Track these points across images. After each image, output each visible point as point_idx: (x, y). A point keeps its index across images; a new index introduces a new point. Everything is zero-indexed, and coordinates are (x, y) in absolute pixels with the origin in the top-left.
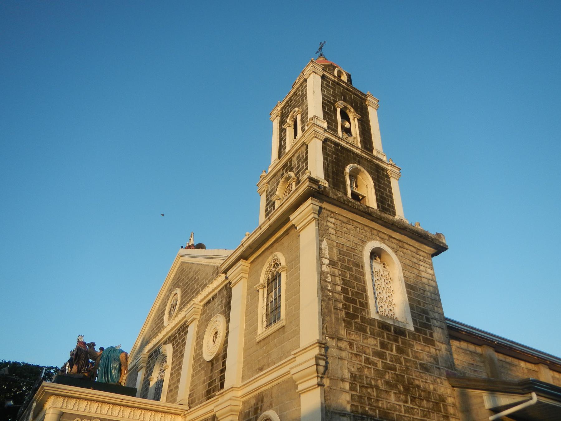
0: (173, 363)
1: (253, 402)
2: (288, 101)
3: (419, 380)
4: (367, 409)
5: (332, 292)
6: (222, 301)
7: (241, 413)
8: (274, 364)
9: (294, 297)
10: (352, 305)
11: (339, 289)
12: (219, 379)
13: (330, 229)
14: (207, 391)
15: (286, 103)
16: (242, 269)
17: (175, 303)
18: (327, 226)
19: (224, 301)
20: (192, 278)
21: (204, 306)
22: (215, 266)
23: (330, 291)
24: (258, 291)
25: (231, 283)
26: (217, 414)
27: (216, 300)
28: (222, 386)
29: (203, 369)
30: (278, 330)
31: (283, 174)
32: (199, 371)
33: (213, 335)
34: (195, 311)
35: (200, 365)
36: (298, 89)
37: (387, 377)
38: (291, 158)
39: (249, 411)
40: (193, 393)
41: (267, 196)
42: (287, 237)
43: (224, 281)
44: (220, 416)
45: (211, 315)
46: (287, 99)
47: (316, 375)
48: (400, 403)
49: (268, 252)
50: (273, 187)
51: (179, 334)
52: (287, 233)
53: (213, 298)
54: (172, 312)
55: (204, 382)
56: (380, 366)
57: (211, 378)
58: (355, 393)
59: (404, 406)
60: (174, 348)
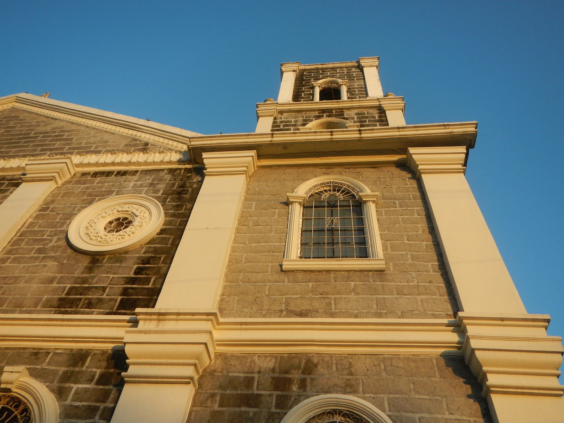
1: (270, 364)
2: (317, 69)
7: (207, 374)
8: (356, 316)
12: (119, 291)
14: (60, 299)
15: (314, 69)
16: (249, 163)
19: (162, 187)
20: (47, 133)
21: (84, 174)
22: (135, 140)
24: (287, 204)
25: (206, 169)
26: (128, 349)
30: (361, 271)
31: (322, 116)
32: (37, 258)
34: (61, 169)
35: (39, 251)
36: (340, 68)
38: (342, 109)
39: (249, 382)
41: (274, 122)
42: (372, 170)
43: (170, 162)
45: (109, 193)
46: (320, 66)
49: (318, 170)
50: (293, 120)
52: (374, 165)
53: (124, 173)
55: (51, 281)
57: (84, 281)
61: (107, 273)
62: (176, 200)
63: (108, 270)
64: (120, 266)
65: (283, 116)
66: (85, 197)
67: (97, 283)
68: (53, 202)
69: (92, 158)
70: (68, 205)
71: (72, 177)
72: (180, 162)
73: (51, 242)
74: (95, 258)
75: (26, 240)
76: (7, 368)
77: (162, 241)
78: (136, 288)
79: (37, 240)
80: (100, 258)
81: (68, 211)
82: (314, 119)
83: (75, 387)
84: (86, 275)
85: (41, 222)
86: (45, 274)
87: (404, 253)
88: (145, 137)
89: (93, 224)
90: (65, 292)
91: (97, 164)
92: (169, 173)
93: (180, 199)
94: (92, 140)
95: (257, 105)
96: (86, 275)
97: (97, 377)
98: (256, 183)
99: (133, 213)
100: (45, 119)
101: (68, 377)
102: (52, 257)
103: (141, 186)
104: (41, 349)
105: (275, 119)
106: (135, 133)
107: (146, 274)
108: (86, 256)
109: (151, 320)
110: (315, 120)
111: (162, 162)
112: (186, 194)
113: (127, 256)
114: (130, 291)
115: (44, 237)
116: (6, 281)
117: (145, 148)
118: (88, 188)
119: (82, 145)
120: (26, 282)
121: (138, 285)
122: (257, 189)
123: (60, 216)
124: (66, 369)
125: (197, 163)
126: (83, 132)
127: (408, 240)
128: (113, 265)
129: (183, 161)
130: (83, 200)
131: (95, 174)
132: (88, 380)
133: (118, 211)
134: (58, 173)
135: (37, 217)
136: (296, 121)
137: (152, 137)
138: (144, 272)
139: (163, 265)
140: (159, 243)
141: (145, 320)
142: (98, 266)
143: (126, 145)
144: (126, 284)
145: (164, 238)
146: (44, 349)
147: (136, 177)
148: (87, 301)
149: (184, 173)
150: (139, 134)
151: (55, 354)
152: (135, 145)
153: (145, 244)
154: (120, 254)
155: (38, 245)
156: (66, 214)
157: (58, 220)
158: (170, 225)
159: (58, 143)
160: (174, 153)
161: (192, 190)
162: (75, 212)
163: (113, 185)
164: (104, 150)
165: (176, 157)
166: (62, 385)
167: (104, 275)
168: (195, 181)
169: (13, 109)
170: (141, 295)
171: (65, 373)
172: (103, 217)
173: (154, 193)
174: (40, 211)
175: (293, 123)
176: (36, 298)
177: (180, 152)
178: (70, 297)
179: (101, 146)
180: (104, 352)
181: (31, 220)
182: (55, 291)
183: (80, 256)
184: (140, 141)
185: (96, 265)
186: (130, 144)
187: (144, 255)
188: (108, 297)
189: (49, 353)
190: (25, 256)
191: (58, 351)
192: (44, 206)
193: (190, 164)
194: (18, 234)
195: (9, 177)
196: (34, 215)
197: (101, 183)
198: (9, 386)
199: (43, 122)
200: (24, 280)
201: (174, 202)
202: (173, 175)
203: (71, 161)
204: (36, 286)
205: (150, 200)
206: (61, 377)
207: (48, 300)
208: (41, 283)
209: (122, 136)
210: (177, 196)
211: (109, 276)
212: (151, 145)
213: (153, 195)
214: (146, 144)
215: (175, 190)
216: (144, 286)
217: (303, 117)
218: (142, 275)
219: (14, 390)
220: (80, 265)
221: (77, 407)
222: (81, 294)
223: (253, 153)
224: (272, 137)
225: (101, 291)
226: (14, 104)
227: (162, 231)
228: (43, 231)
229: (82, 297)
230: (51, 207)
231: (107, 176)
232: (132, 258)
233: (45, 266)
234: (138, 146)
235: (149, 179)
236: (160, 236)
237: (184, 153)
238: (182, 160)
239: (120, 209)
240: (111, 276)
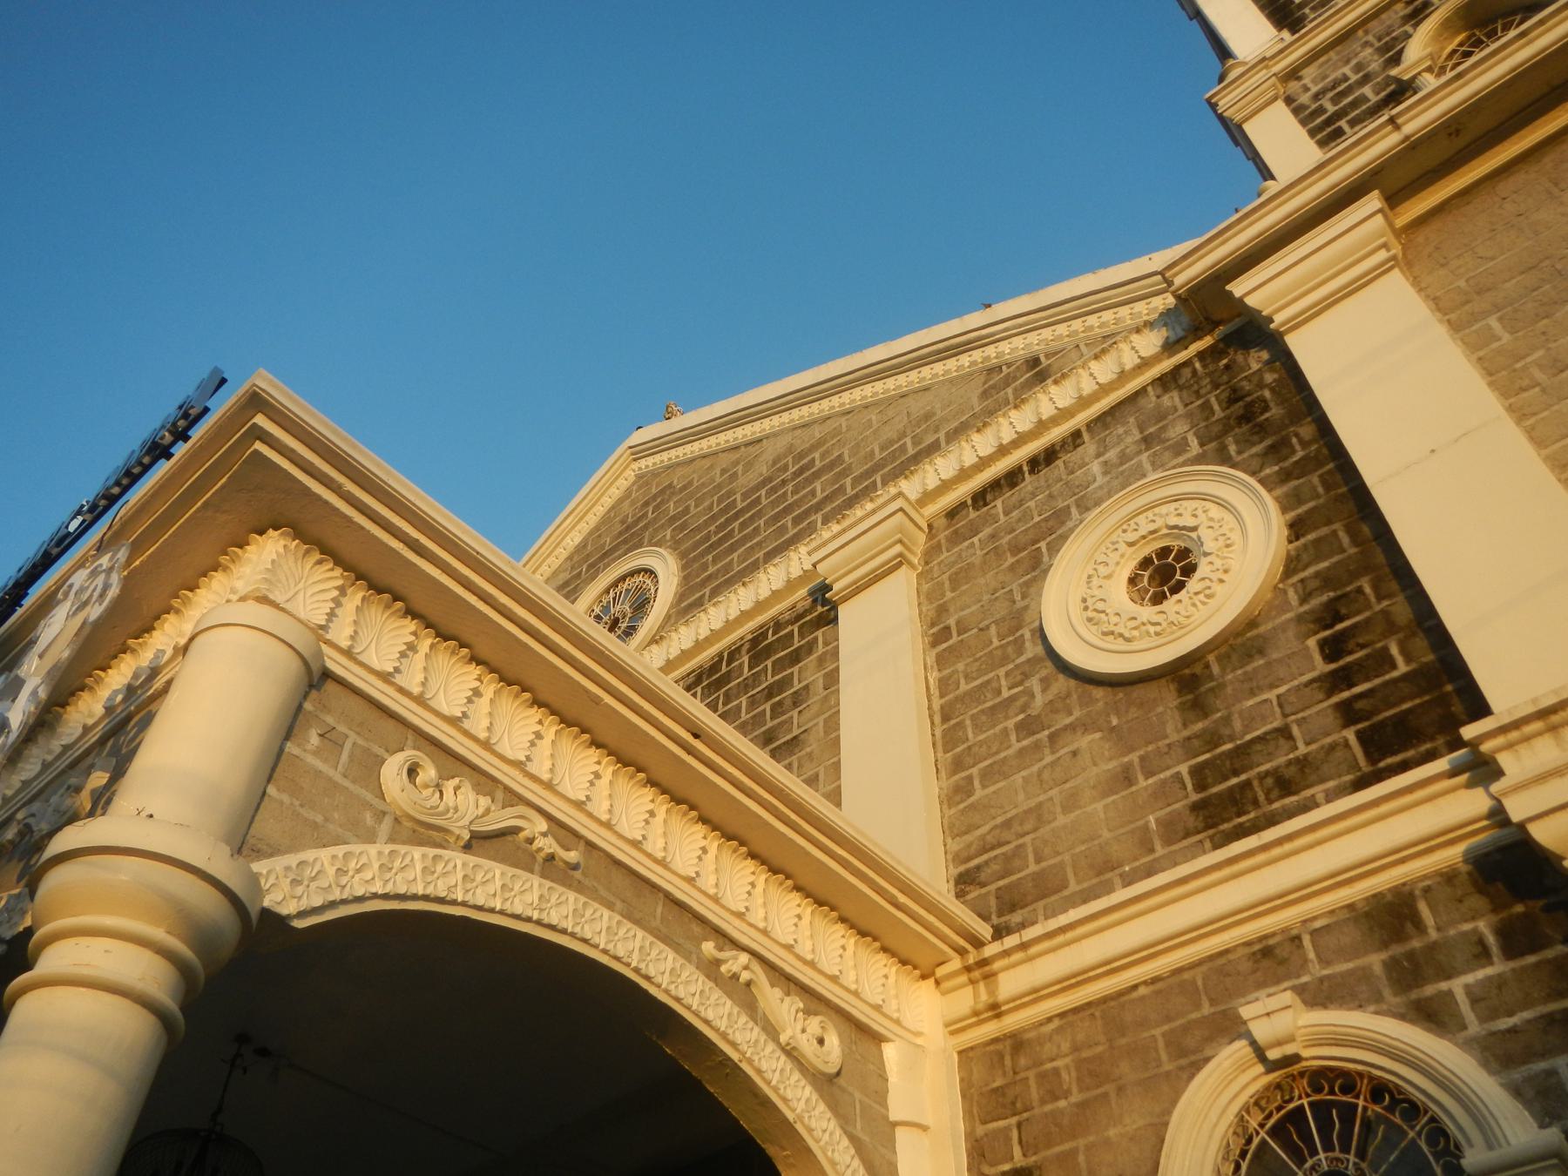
14: (1196, 807)
21: (952, 514)
29: (1084, 726)
32: (1037, 746)
35: (1026, 728)
43: (1145, 364)
45: (1061, 516)
53: (1049, 456)
55: (1126, 778)
61: (1252, 693)
62: (1256, 438)
63: (1246, 686)
64: (1269, 664)
65: (1306, 81)
66: (1011, 560)
67: (1247, 728)
68: (942, 610)
69: (943, 466)
70: (986, 597)
72: (1170, 347)
73: (1033, 696)
74: (1186, 677)
75: (968, 722)
77: (1320, 549)
78: (1371, 692)
79: (993, 708)
80: (1198, 669)
81: (1001, 609)
82: (1408, 28)
85: (960, 666)
86: (1095, 770)
88: (1015, 348)
89: (1100, 606)
90: (1190, 786)
91: (964, 474)
92: (1166, 389)
93: (1262, 430)
94: (889, 433)
95: (1208, 101)
97: (1491, 940)
98: (1442, 272)
99: (1175, 527)
100: (734, 456)
102: (1072, 728)
103: (1124, 458)
104: (1266, 937)
105: (1289, 101)
106: (977, 355)
107: (1363, 646)
108: (1154, 684)
109: (1527, 739)
110: (1416, 26)
111: (1123, 376)
112: (1266, 409)
113: (1262, 629)
114: (1359, 705)
115: (1006, 694)
116: (1017, 828)
117: (1038, 371)
118: (993, 536)
119: (878, 456)
120: (1066, 809)
121: (1368, 679)
122: (1462, 283)
123: (993, 629)
124: (1384, 955)
125: (1217, 324)
126: (849, 428)
128: (1249, 668)
129: (1178, 341)
130: (1012, 568)
131: (980, 498)
132: (1476, 956)
133: (1131, 544)
134: (900, 541)
135: (941, 661)
136: (1359, 67)
137: (1033, 338)
138: (1351, 645)
139: (1385, 603)
140: (1318, 558)
141: (1510, 746)
142: (1212, 689)
143: (985, 394)
145: (1317, 541)
146: (1273, 934)
147: (1089, 447)
148: (1269, 781)
149: (1204, 366)
150: (991, 351)
151: (1314, 933)
152: (1007, 381)
153: (1282, 580)
154: (1238, 634)
155: (1007, 718)
156: (1003, 619)
157: (996, 643)
158: (1300, 502)
159: (818, 485)
160: (1135, 337)
161: (1272, 390)
162: (1020, 604)
163: (1051, 496)
164: (942, 435)
165: (1150, 343)
166: (1414, 995)
167: (1250, 703)
168: (1255, 366)
169: (642, 479)
170: (1403, 700)
172: (1108, 577)
173: (1178, 454)
174: (934, 644)
175: (1354, 78)
176: (1132, 832)
177: (1150, 325)
178: (1215, 790)
179: (926, 431)
180: (1449, 876)
181: (933, 677)
182: (1161, 794)
183: (1138, 692)
184: (1009, 365)
185: (1202, 689)
186: (992, 387)
187: (1306, 607)
188: (1314, 747)
189: (1298, 938)
190: (1002, 755)
191: (1318, 924)
192: (935, 630)
193: (1200, 338)
194: (937, 719)
195: (787, 616)
196: (931, 660)
197: (1015, 508)
198: (1289, 1049)
199: (737, 463)
200: (1059, 809)
201: (1254, 444)
202: (1180, 388)
203: (907, 499)
204: (1099, 806)
205: (1188, 474)
206: (1390, 978)
208: (1105, 795)
209: (951, 381)
210: (1245, 428)
211: (1265, 697)
212: (1047, 356)
213: (1181, 459)
214: (1035, 362)
215: (1228, 418)
216: (1387, 677)
217: (1367, 44)
218: (1351, 653)
219: (1305, 1053)
220: (1160, 709)
221: (1513, 1031)
222: (1236, 773)
223: (1373, 201)
224: (1398, 128)
225: (1282, 741)
226: (635, 466)
227: (1297, 529)
228: (988, 682)
229: (1243, 777)
230: (952, 622)
231: (1013, 485)
232: (1283, 628)
233: (1074, 753)
234: (1015, 379)
235: (1128, 434)
236: (1302, 541)
237: (1167, 317)
238: (1173, 338)
239: (1132, 537)
240: (1272, 695)
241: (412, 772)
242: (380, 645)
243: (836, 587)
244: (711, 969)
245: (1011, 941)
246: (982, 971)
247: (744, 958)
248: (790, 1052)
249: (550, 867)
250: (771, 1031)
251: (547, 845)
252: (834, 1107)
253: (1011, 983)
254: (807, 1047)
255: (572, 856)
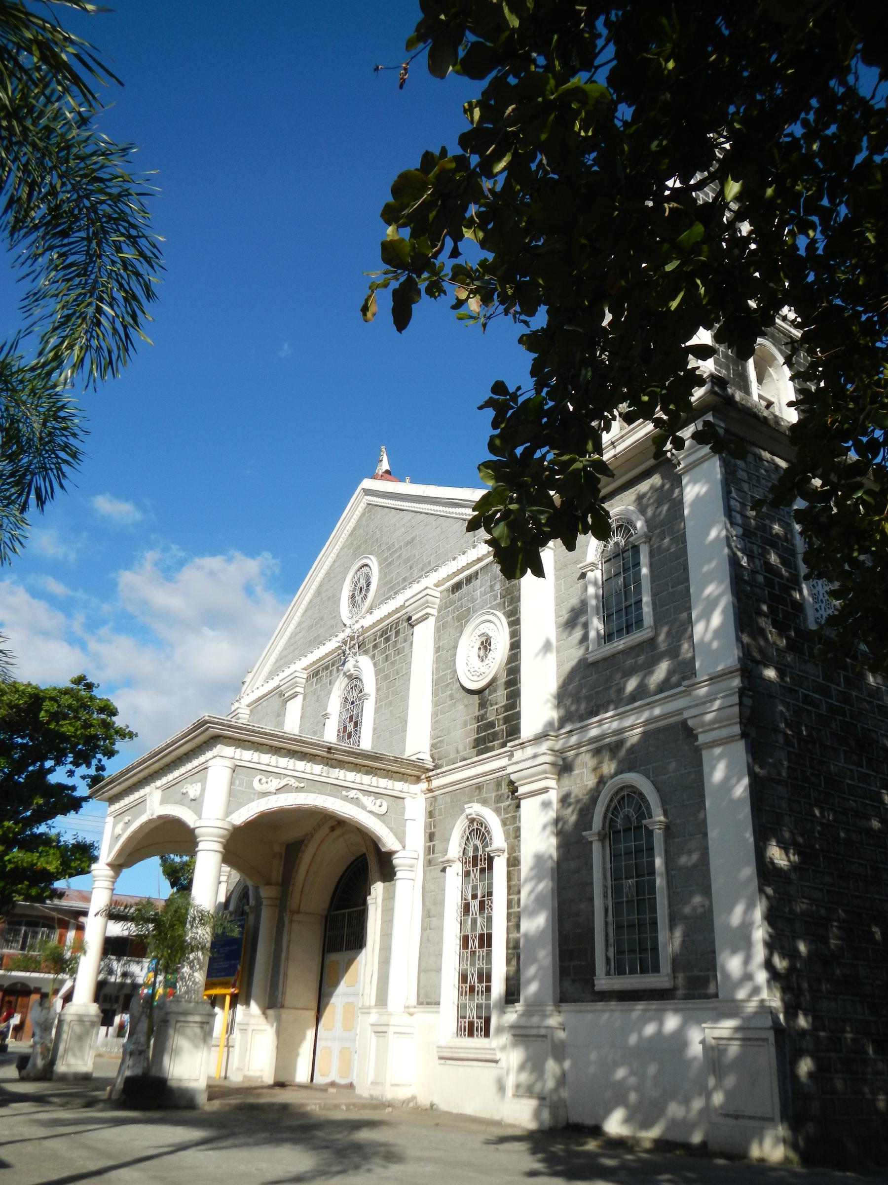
0: (378, 690)
3: (876, 732)
4: (808, 774)
5: (751, 586)
6: (491, 586)
9: (671, 590)
10: (781, 607)
11: (760, 578)
13: (740, 471)
14: (475, 740)
17: (363, 582)
18: (735, 465)
19: (498, 587)
23: (746, 582)
27: (476, 583)
28: (514, 731)
33: (478, 644)
35: (451, 697)
37: (833, 725)
40: (440, 741)
44: (520, 780)
47: (738, 720)
48: (851, 767)
51: (387, 640)
53: (469, 579)
54: (358, 598)
55: (465, 724)
56: (823, 710)
58: (791, 750)
59: (857, 771)
60: (375, 665)
71: (441, 601)
76: (466, 806)
83: (503, 805)
84: (482, 712)
87: (668, 607)
96: (482, 712)
101: (499, 799)
115: (449, 681)
127: (672, 587)
144: (506, 711)
147: (478, 581)
171: (496, 796)
207: (469, 742)
239: (479, 633)
241: (260, 780)
242: (247, 755)
243: (414, 618)
244: (346, 798)
245: (439, 771)
246: (429, 779)
247: (355, 791)
248: (370, 812)
249: (298, 789)
250: (364, 808)
251: (296, 784)
252: (383, 822)
253: (435, 783)
254: (376, 809)
255: (302, 785)
